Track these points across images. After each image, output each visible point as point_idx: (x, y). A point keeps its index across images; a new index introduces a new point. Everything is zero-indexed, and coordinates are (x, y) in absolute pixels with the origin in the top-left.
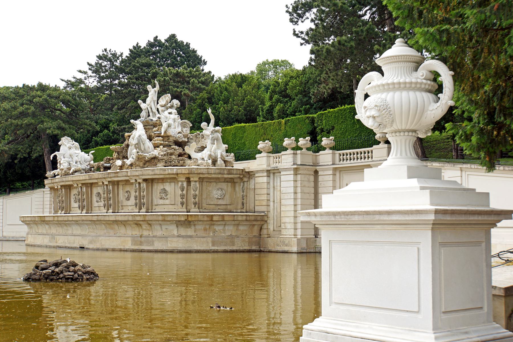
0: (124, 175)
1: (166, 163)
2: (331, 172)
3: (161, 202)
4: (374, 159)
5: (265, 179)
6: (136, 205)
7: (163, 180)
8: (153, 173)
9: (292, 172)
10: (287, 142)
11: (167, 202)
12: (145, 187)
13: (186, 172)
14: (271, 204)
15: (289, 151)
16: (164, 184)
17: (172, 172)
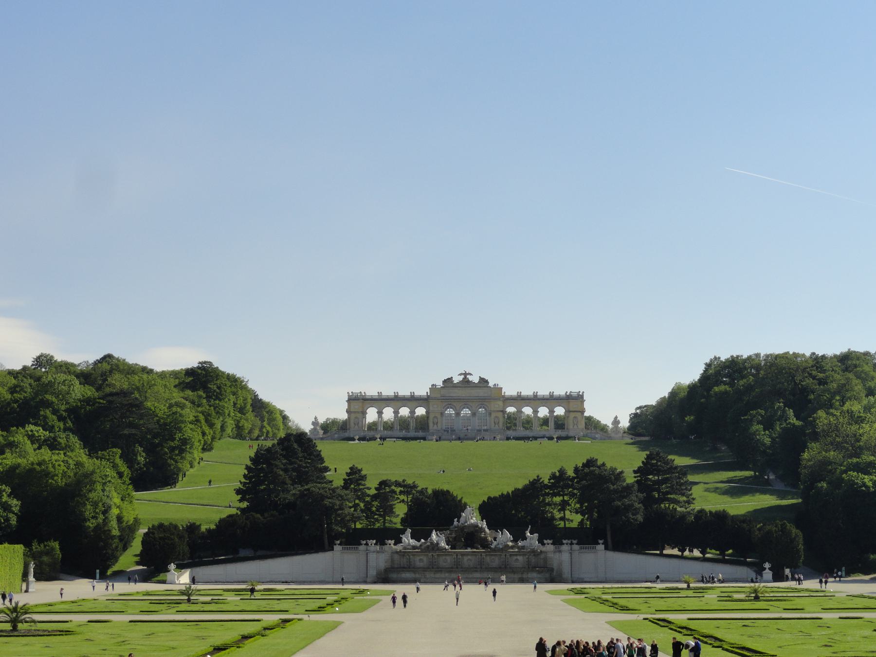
10: (564, 541)
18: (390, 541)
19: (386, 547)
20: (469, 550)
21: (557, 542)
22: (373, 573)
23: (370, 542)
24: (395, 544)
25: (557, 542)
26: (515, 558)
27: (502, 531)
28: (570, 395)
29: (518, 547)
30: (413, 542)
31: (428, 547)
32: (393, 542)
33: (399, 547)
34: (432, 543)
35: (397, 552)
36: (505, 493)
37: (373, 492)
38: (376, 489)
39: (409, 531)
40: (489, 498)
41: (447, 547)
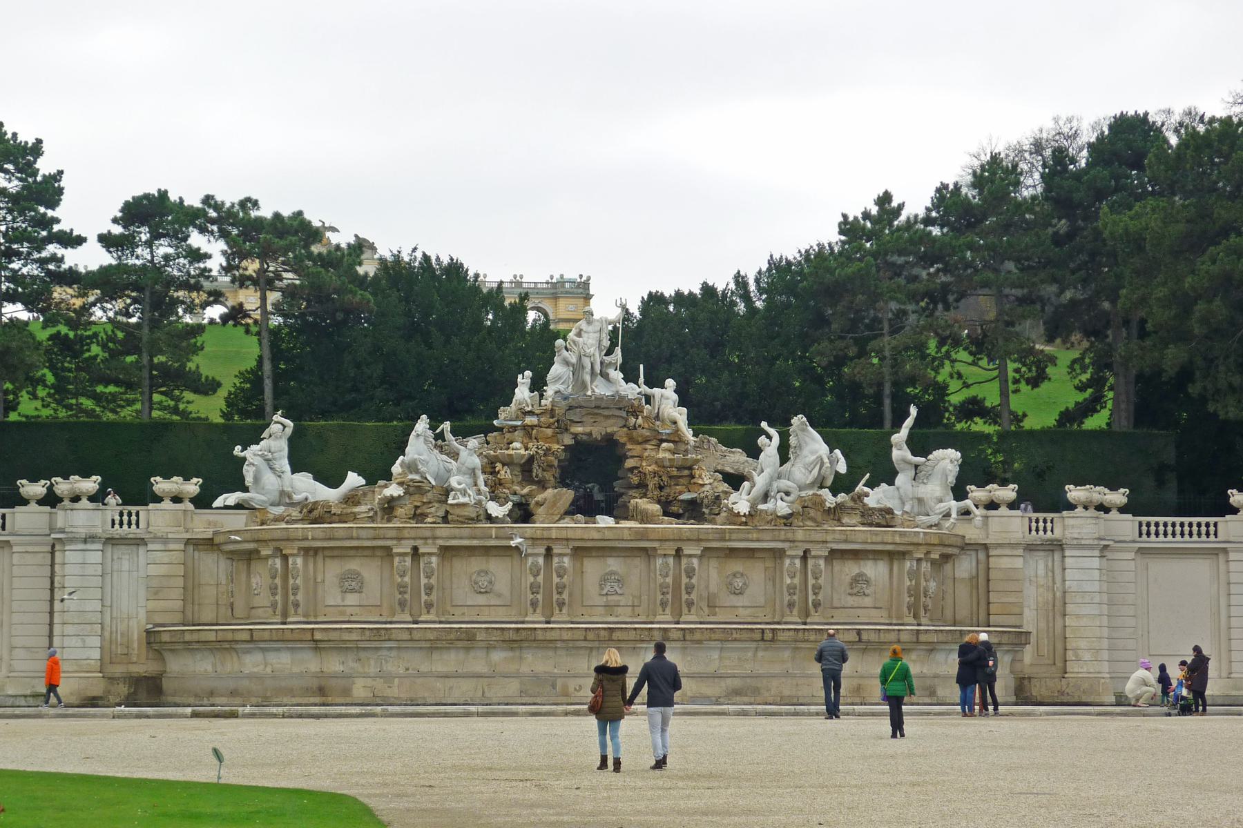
0: (782, 537)
1: (863, 516)
2: (1131, 555)
3: (851, 601)
4: (1220, 538)
5: (1019, 563)
6: (791, 605)
7: (856, 555)
8: (879, 539)
9: (1097, 553)
10: (1075, 493)
11: (867, 601)
12: (822, 567)
13: (936, 542)
14: (1027, 612)
15: (1080, 510)
16: (862, 562)
17: (915, 540)
18: (174, 485)
19: (157, 518)
20: (605, 521)
21: (1043, 496)
22: (81, 652)
23: (62, 486)
24: (203, 501)
25: (1043, 496)
26: (851, 569)
27: (782, 423)
28: (562, 282)
29: (868, 516)
30: (306, 486)
31: (389, 506)
32: (192, 487)
33: (227, 517)
34: (414, 489)
35: (209, 544)
36: (723, 282)
37: (90, 258)
38: (106, 240)
39: (280, 428)
40: (654, 301)
41: (495, 509)
